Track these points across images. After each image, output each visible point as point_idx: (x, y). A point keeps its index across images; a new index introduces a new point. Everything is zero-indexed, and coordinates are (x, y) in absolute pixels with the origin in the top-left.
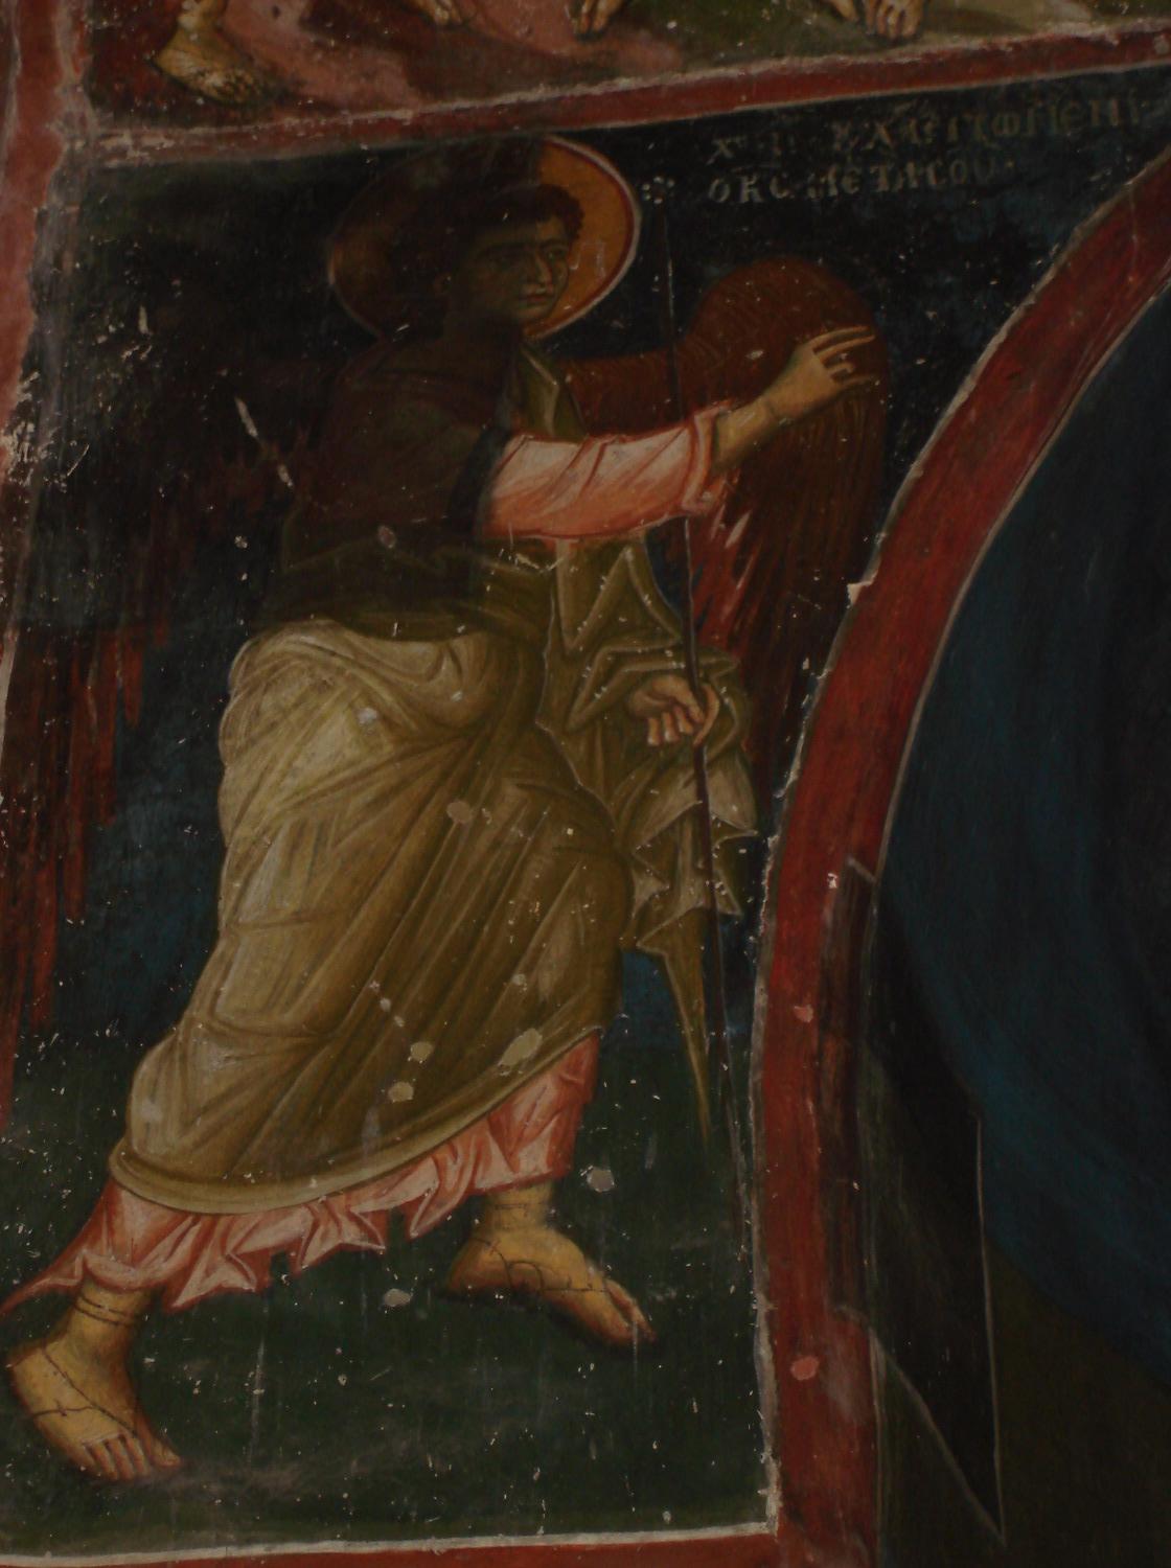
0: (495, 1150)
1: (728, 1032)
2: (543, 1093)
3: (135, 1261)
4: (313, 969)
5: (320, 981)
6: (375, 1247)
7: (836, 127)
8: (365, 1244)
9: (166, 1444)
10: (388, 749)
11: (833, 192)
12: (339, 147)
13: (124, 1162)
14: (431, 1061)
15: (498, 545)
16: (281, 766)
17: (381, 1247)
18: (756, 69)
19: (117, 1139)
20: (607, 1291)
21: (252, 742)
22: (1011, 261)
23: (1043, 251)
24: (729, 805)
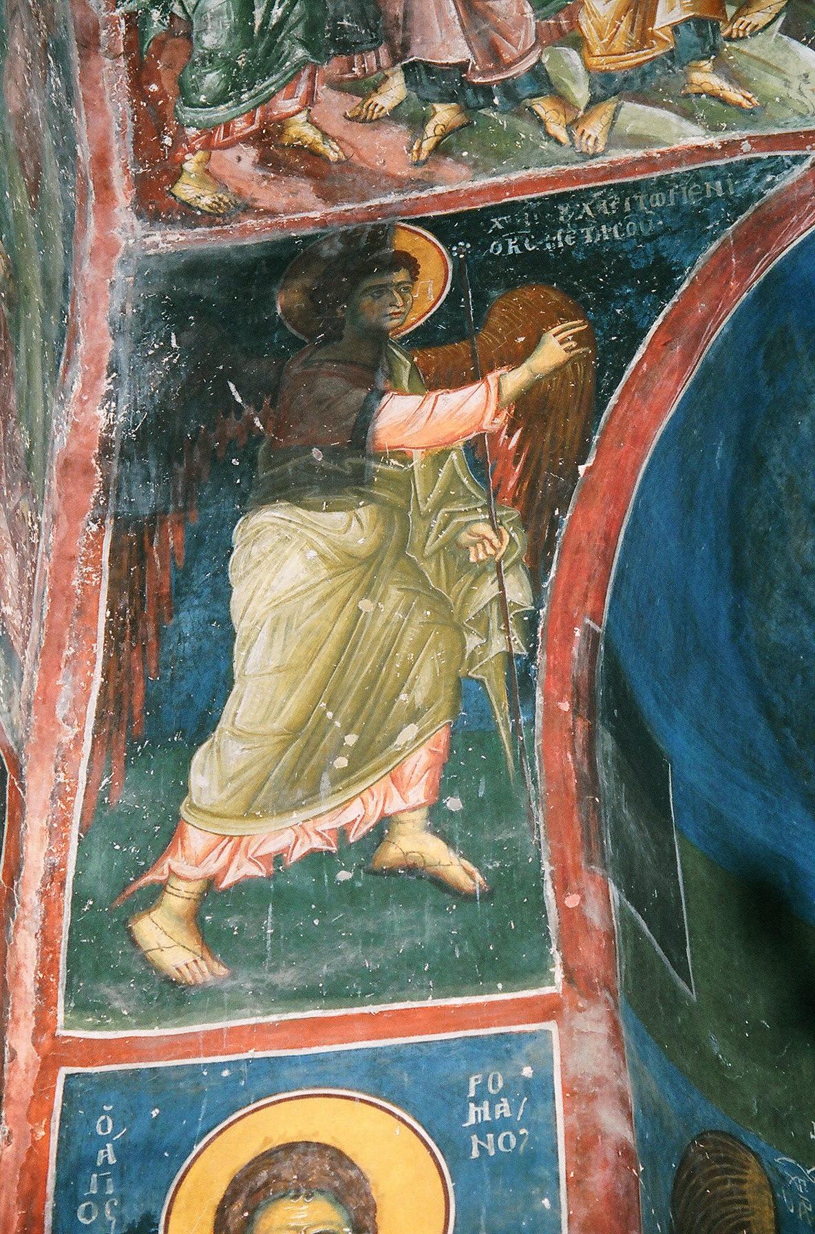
0: (394, 789)
4: (288, 698)
7: (560, 207)
8: (326, 848)
9: (219, 962)
11: (561, 245)
12: (278, 235)
14: (357, 744)
15: (378, 456)
16: (264, 585)
17: (334, 849)
18: (514, 177)
21: (248, 573)
22: (662, 278)
23: (681, 272)
24: (518, 592)
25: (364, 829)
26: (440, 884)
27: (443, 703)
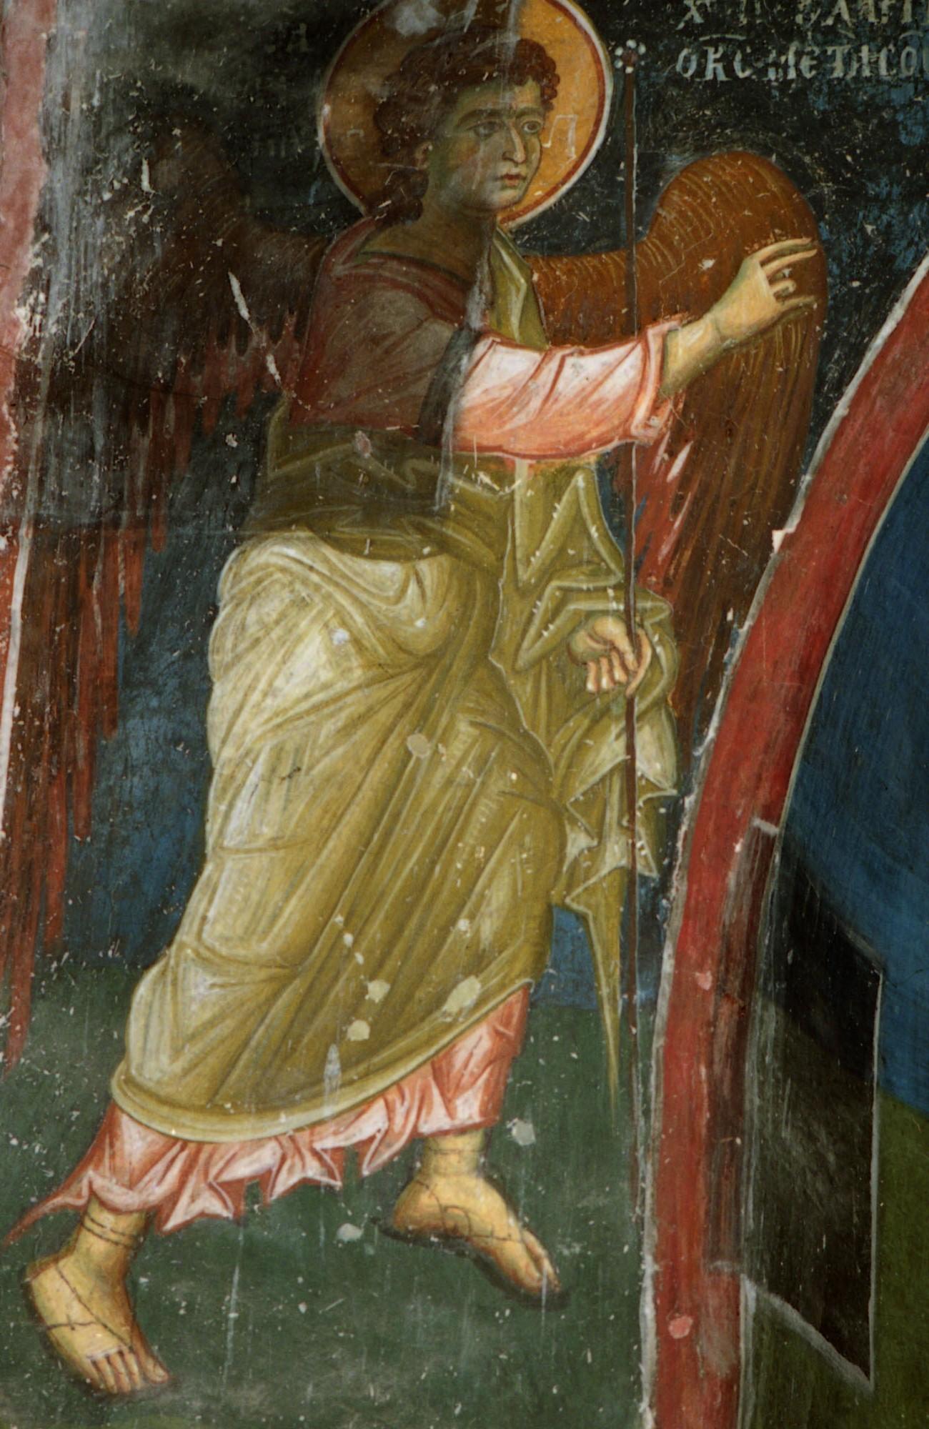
0: (435, 1091)
1: (639, 995)
2: (476, 1045)
3: (131, 1186)
4: (287, 899)
5: (294, 911)
6: (332, 1182)
8: (325, 1180)
10: (358, 674)
11: (792, 74)
13: (125, 1087)
14: (387, 999)
15: (464, 462)
16: (262, 685)
17: (338, 1184)
19: (119, 1061)
20: (523, 1241)
21: (238, 658)
24: (655, 762)
25: (385, 1156)
26: (489, 1267)
27: (520, 952)
